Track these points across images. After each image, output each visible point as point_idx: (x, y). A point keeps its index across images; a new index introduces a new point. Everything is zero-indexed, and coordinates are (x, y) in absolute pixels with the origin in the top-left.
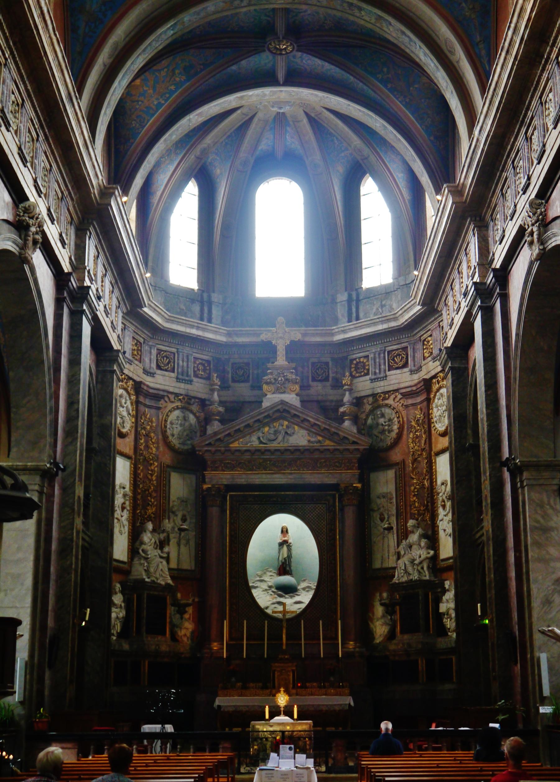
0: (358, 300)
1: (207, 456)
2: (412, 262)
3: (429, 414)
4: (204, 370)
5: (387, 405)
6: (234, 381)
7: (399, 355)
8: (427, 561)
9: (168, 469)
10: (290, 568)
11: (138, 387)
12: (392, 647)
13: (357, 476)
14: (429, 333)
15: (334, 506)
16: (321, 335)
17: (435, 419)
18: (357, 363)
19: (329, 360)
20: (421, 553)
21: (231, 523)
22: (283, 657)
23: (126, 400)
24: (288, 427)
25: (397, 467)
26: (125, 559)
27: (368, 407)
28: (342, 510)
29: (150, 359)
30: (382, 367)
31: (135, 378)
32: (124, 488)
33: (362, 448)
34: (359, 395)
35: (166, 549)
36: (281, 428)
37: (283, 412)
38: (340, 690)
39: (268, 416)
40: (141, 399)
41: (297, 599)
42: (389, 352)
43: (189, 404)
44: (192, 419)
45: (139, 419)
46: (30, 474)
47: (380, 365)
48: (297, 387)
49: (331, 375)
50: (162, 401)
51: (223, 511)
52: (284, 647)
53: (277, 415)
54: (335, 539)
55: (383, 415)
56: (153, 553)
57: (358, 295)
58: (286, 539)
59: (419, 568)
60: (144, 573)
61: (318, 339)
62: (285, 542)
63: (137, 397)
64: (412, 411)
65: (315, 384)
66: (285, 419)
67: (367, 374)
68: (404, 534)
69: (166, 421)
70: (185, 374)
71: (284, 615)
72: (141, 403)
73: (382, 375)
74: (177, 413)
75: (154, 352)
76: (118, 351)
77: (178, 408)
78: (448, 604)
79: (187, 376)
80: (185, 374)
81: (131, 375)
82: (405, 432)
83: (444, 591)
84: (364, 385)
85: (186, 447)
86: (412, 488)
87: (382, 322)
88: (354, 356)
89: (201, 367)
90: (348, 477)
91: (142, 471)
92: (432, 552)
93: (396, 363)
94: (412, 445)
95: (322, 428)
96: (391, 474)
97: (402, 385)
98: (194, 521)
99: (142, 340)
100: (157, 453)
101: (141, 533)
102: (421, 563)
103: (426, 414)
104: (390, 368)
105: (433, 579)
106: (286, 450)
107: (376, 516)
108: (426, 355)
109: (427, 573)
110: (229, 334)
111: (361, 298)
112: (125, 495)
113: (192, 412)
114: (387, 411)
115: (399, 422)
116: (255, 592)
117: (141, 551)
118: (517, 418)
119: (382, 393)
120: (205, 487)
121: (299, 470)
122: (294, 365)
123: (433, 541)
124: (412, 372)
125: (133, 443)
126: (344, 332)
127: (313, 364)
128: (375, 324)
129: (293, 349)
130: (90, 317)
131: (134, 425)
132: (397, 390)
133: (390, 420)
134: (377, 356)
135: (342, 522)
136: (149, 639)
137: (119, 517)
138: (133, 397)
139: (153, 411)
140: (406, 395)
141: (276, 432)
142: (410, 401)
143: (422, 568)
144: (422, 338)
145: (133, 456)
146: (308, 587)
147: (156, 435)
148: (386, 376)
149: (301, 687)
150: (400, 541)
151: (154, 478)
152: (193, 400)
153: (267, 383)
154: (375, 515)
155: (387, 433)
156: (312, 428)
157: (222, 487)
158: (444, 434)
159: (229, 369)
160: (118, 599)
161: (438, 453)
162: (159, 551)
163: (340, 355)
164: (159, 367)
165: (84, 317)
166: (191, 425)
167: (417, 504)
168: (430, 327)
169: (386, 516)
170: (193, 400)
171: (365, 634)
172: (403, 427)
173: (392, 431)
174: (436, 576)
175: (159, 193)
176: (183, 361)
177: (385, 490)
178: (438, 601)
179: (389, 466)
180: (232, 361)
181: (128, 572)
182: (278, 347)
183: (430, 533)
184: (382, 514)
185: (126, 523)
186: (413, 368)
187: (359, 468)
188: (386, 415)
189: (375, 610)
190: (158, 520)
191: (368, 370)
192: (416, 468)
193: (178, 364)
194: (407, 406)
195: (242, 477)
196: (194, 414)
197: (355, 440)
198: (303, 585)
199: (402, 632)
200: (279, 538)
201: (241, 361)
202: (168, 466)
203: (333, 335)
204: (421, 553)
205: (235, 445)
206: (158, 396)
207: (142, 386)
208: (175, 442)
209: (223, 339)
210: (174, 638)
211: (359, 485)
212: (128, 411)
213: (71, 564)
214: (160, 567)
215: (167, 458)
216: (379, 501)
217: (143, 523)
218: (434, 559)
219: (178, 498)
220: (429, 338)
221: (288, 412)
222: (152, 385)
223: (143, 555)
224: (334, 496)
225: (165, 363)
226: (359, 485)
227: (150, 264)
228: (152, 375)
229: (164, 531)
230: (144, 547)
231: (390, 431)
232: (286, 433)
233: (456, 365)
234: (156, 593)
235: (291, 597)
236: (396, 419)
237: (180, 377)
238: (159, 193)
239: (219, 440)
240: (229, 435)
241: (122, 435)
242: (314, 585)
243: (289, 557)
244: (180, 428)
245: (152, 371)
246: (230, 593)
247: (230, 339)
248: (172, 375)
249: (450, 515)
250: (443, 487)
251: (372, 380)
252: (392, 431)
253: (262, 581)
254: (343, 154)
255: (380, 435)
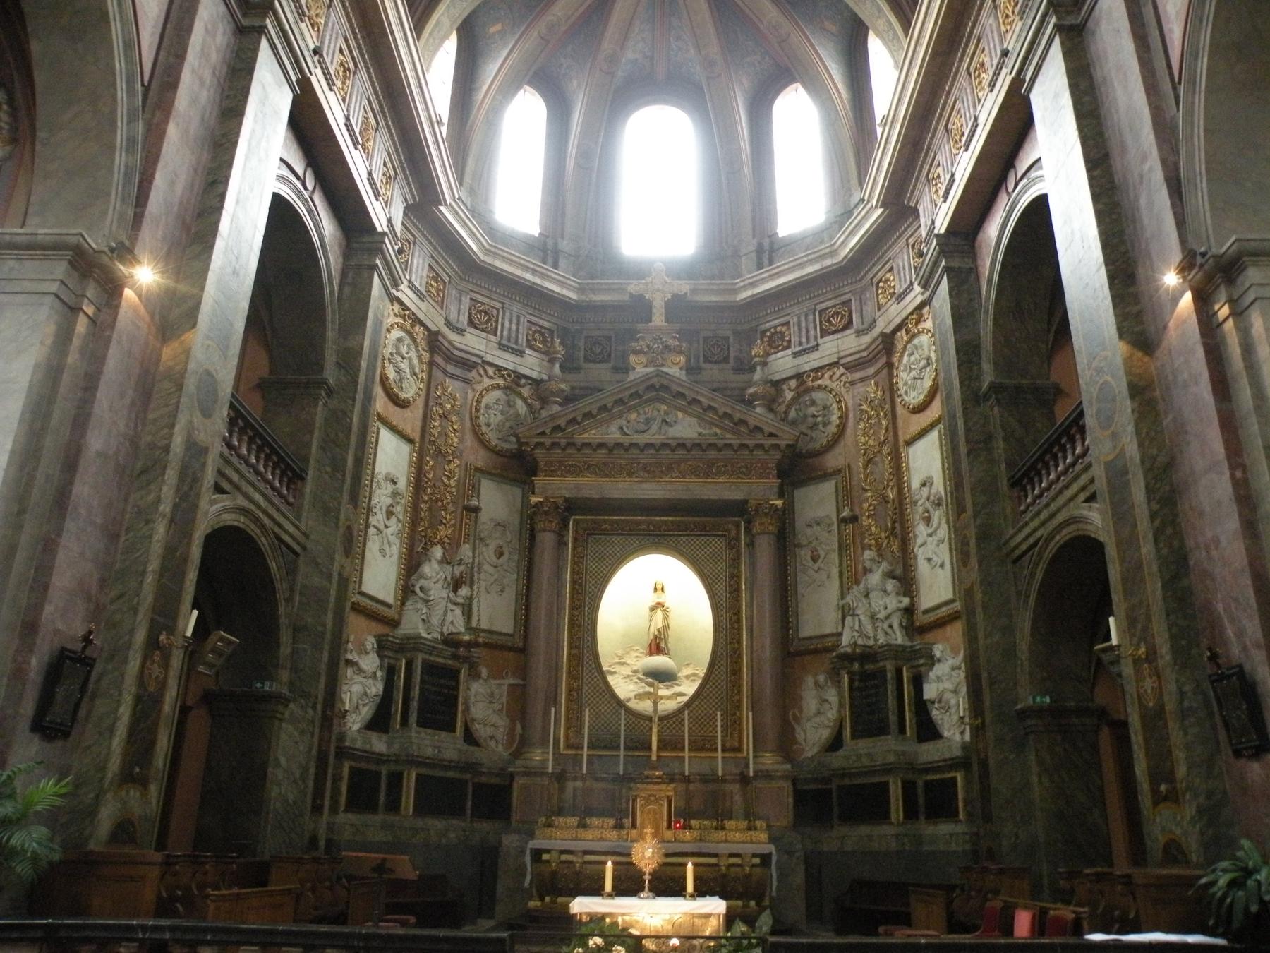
0: (772, 251)
1: (539, 454)
2: (854, 181)
3: (892, 385)
4: (544, 342)
5: (819, 386)
6: (587, 360)
7: (838, 313)
8: (899, 614)
9: (478, 475)
10: (666, 643)
11: (434, 341)
12: (837, 760)
13: (776, 490)
14: (888, 266)
15: (737, 539)
16: (719, 292)
17: (902, 391)
18: (772, 335)
19: (729, 333)
20: (889, 602)
21: (575, 563)
22: (651, 773)
23: (408, 347)
24: (666, 413)
25: (839, 477)
26: (390, 600)
27: (789, 395)
28: (751, 544)
29: (459, 310)
30: (812, 333)
31: (429, 325)
32: (394, 483)
33: (783, 443)
34: (777, 377)
35: (464, 591)
36: (656, 413)
37: (658, 390)
38: (751, 833)
39: (636, 395)
40: (439, 360)
41: (677, 689)
42: (820, 312)
43: (518, 385)
44: (521, 407)
45: (432, 389)
46: (46, 258)
47: (807, 331)
48: (682, 359)
49: (732, 354)
50: (474, 373)
51: (561, 543)
52: (654, 758)
53: (653, 394)
54: (738, 590)
55: (813, 403)
56: (438, 592)
57: (772, 243)
58: (660, 600)
59: (886, 626)
60: (420, 625)
61: (714, 298)
62: (660, 605)
63: (432, 356)
64: (860, 388)
65: (707, 366)
66: (662, 401)
67: (788, 347)
68: (851, 577)
69: (478, 402)
70: (513, 340)
71: (655, 704)
72: (438, 366)
73: (813, 343)
74: (497, 394)
75: (466, 301)
76: (384, 234)
77: (498, 387)
78: (945, 682)
79: (516, 343)
80: (513, 340)
81: (421, 316)
82: (851, 423)
83: (932, 661)
84: (783, 363)
85: (506, 446)
86: (865, 505)
87: (811, 261)
88: (767, 325)
89: (538, 337)
90: (761, 489)
91: (433, 468)
92: (906, 601)
93: (831, 324)
94: (863, 440)
95: (721, 413)
96: (827, 489)
97: (842, 354)
98: (516, 557)
99: (447, 279)
100: (461, 447)
101: (424, 562)
102: (887, 617)
103: (887, 387)
104: (825, 333)
105: (908, 644)
106: (665, 445)
107: (805, 554)
108: (883, 301)
109: (898, 633)
110: (581, 290)
111: (776, 247)
112: (395, 494)
113: (520, 395)
114: (818, 396)
115: (840, 409)
116: (610, 678)
117: (417, 590)
118: (1200, 165)
119: (812, 371)
120: (534, 500)
121: (683, 477)
122: (677, 326)
123: (906, 581)
124: (859, 333)
125: (419, 424)
126: (753, 285)
127: (706, 339)
128: (801, 266)
129: (676, 307)
130: (294, 79)
131: (423, 393)
132: (835, 364)
133: (825, 408)
134: (803, 319)
135: (753, 566)
136: (423, 735)
137: (382, 527)
138: (426, 356)
139: (458, 384)
140: (850, 368)
141: (648, 422)
142: (858, 375)
143: (891, 626)
144: (875, 281)
145: (417, 440)
146: (694, 675)
147: (462, 421)
148: (818, 345)
149: (684, 828)
150: (845, 590)
151: (453, 483)
152: (523, 381)
153: (636, 353)
154: (803, 553)
155: (821, 427)
156: (704, 412)
157: (560, 501)
158: (920, 409)
159: (581, 344)
160: (370, 662)
161: (909, 443)
162: (452, 595)
163: (746, 327)
164: (471, 323)
165: (264, 43)
166: (518, 415)
167: (873, 529)
168: (890, 254)
169: (822, 554)
170: (523, 381)
171: (786, 744)
172: (847, 416)
173: (829, 423)
174: (911, 640)
175: (485, 88)
176: (511, 322)
177: (821, 513)
178: (918, 682)
179: (825, 476)
180: (585, 333)
181: (395, 624)
182: (654, 303)
183: (899, 571)
184: (814, 550)
185: (396, 542)
186: (861, 327)
187: (781, 474)
188: (818, 402)
189: (804, 704)
190: (452, 546)
191: (789, 341)
192: (872, 473)
193: (503, 325)
194: (852, 383)
195: (590, 486)
196: (524, 400)
197: (774, 431)
198: (686, 671)
199: (854, 736)
200: (653, 599)
201: (597, 333)
202: (477, 469)
203: (736, 291)
204: (889, 602)
205: (582, 438)
206: (468, 364)
207: (440, 338)
208: (492, 437)
209: (573, 296)
210: (470, 738)
211: (779, 503)
212: (412, 367)
213: (158, 500)
214: (450, 617)
215: (479, 458)
216: (809, 531)
217: (426, 549)
218: (909, 611)
219: (492, 520)
220: (888, 275)
221: (665, 388)
222: (458, 345)
223: (421, 595)
224: (738, 526)
225: (481, 320)
226: (779, 503)
227: (467, 179)
228: (461, 332)
229: (460, 562)
230: (422, 582)
231: (825, 424)
232: (664, 421)
233: (956, 263)
234: (441, 660)
235: (668, 687)
236: (835, 405)
237: (505, 342)
238: (485, 88)
239: (557, 428)
240: (573, 421)
241: (401, 404)
242: (702, 672)
243: (666, 627)
244: (500, 417)
245: (459, 326)
246: (569, 672)
247: (583, 297)
248: (493, 338)
249: (943, 532)
250: (925, 490)
251: (796, 355)
252: (829, 423)
253: (623, 664)
254: (748, 59)
255: (809, 432)
